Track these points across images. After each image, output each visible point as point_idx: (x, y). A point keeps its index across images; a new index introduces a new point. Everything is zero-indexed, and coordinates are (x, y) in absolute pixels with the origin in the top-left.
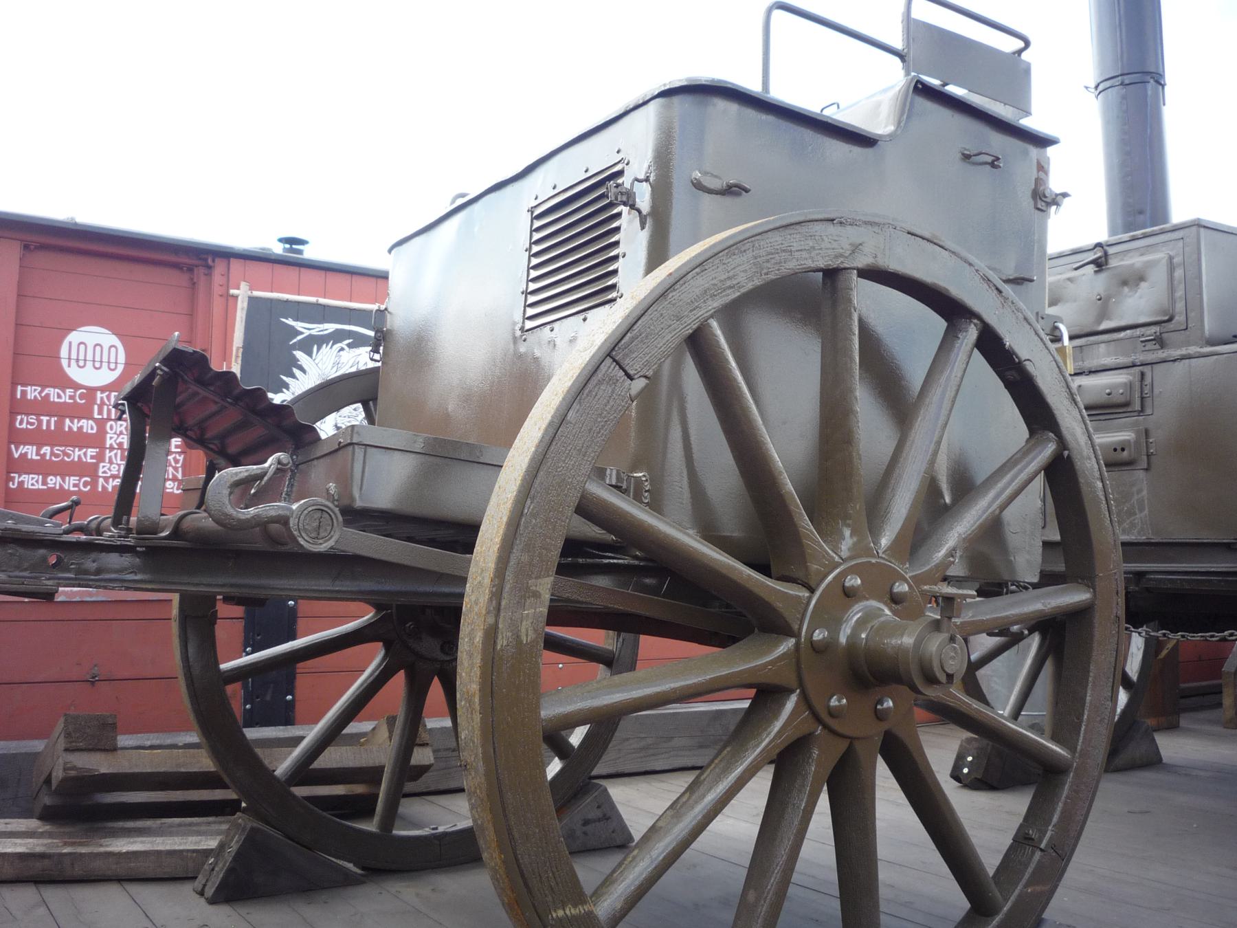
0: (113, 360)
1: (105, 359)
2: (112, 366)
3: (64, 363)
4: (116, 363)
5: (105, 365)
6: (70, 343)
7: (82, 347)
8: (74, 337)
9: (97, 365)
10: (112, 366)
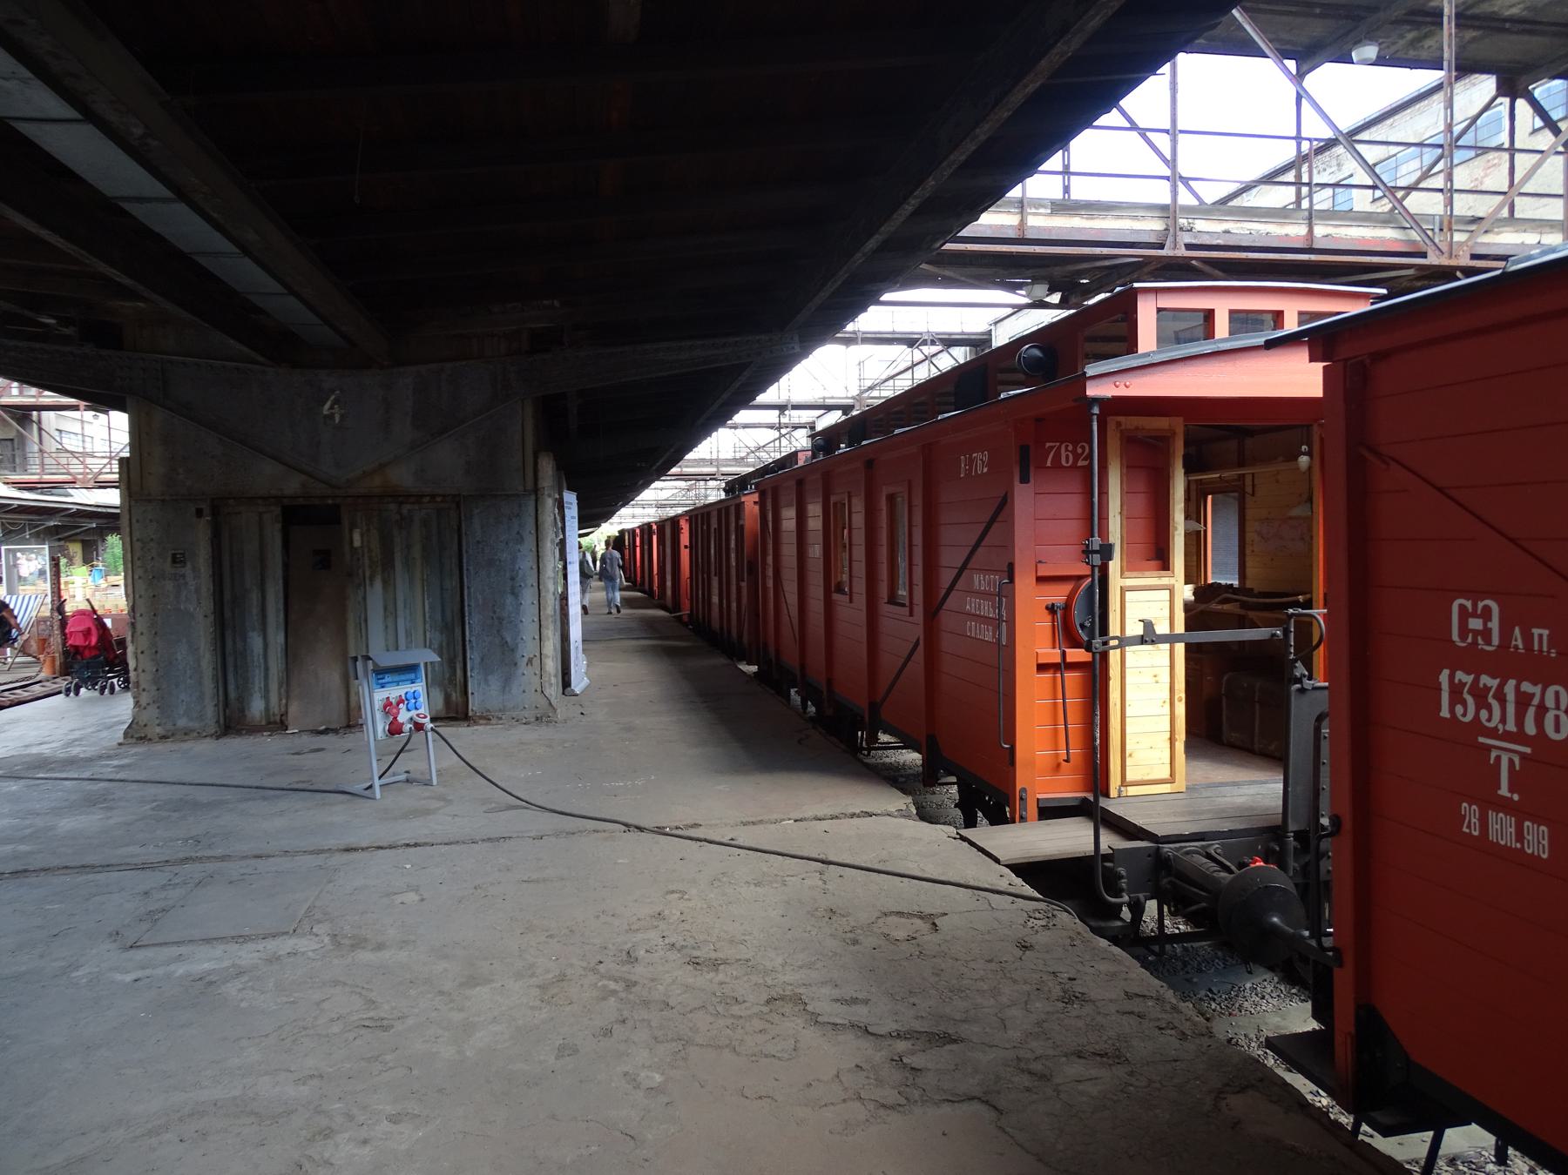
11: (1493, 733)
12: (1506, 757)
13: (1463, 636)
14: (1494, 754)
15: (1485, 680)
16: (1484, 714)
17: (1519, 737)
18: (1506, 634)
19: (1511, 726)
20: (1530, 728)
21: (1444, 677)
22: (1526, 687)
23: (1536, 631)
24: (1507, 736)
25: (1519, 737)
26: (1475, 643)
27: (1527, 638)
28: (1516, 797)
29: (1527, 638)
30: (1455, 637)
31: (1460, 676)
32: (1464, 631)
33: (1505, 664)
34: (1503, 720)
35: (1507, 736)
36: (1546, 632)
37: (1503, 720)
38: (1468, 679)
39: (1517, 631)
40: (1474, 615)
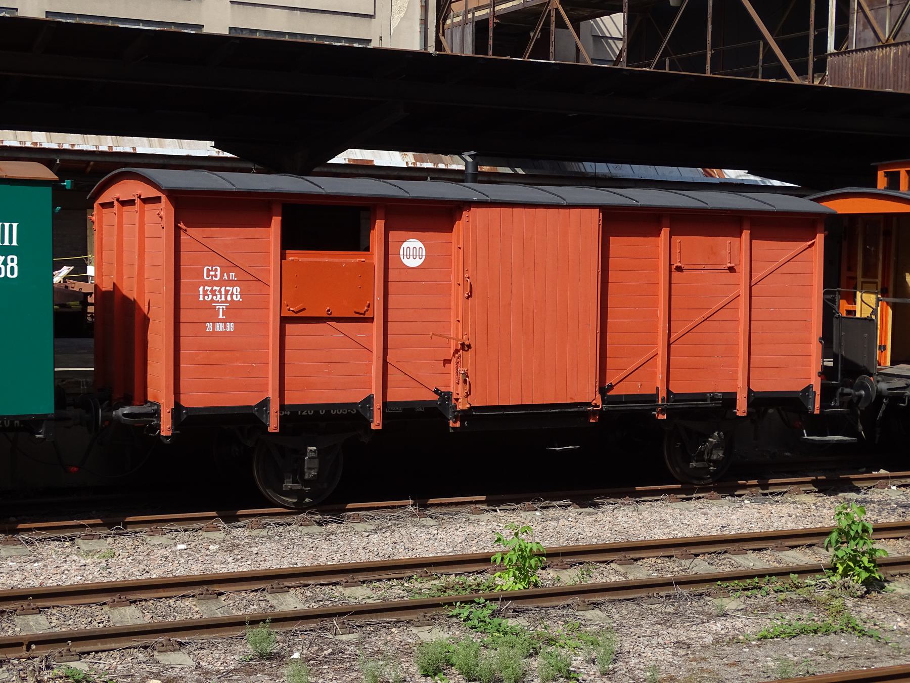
0: (420, 254)
1: (417, 254)
2: (421, 257)
3: (402, 257)
4: (422, 255)
5: (418, 257)
6: (404, 248)
7: (408, 249)
8: (405, 245)
9: (415, 257)
10: (421, 257)
11: (218, 302)
12: (221, 308)
13: (208, 277)
14: (217, 307)
15: (215, 288)
16: (214, 297)
17: (226, 301)
18: (222, 275)
19: (223, 299)
20: (229, 298)
21: (201, 289)
22: (228, 288)
23: (231, 274)
24: (222, 302)
25: (226, 301)
26: (212, 278)
27: (228, 276)
28: (224, 317)
29: (228, 276)
30: (205, 277)
31: (206, 288)
32: (208, 275)
33: (221, 283)
34: (221, 298)
35: (222, 302)
36: (234, 274)
37: (221, 298)
38: (209, 288)
39: (225, 274)
40: (212, 271)
